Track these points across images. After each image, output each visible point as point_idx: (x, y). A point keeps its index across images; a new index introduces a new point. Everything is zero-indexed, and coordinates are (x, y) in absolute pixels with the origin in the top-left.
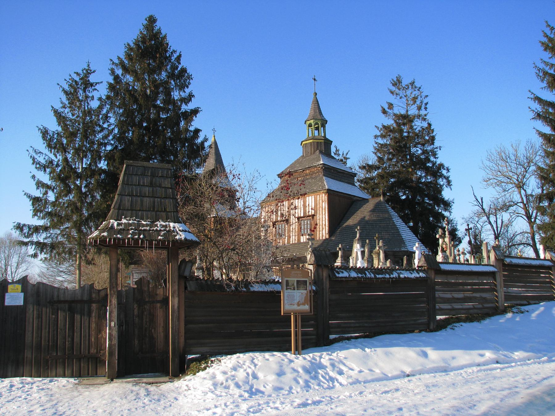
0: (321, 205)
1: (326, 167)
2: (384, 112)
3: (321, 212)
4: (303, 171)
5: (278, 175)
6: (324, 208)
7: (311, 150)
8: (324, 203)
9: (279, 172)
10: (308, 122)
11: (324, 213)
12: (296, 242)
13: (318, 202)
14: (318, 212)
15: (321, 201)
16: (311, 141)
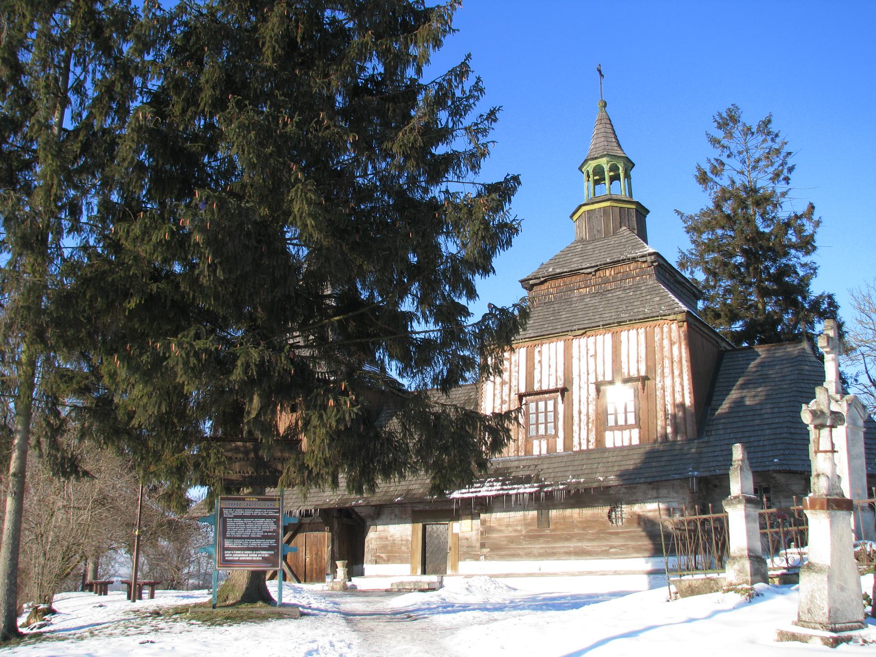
0: (666, 352)
1: (662, 262)
2: (703, 179)
3: (667, 371)
4: (596, 271)
5: (522, 281)
6: (676, 359)
7: (607, 226)
8: (675, 348)
9: (524, 277)
10: (591, 166)
11: (677, 372)
12: (591, 447)
13: (657, 344)
14: (659, 371)
15: (666, 342)
16: (608, 204)
